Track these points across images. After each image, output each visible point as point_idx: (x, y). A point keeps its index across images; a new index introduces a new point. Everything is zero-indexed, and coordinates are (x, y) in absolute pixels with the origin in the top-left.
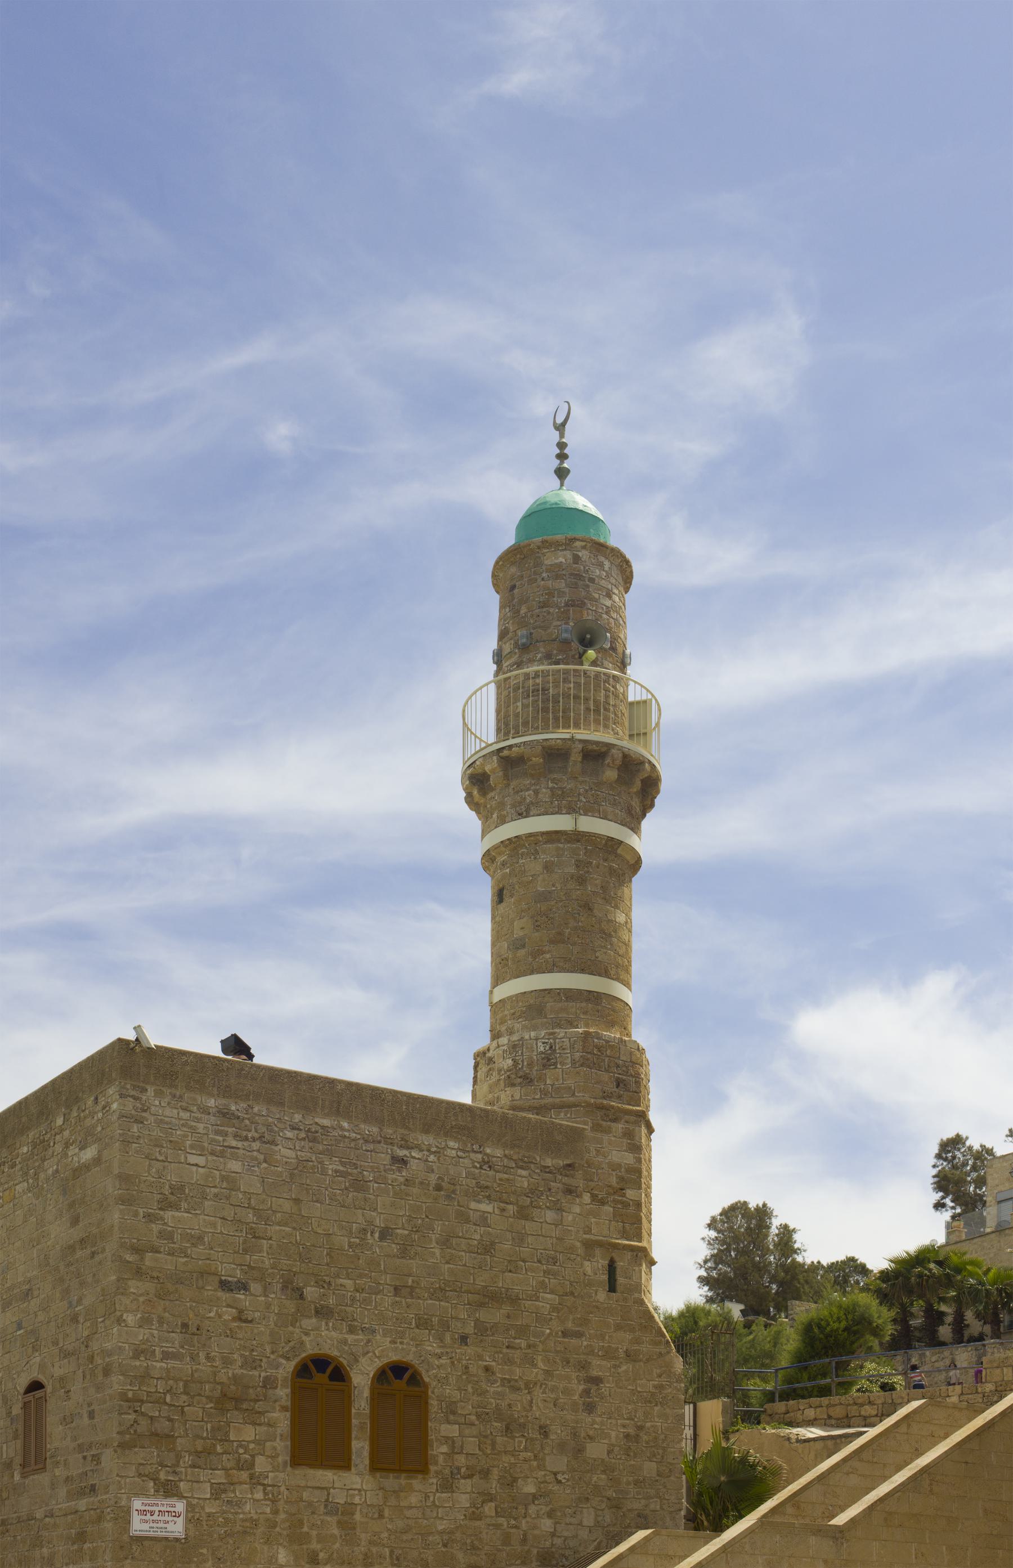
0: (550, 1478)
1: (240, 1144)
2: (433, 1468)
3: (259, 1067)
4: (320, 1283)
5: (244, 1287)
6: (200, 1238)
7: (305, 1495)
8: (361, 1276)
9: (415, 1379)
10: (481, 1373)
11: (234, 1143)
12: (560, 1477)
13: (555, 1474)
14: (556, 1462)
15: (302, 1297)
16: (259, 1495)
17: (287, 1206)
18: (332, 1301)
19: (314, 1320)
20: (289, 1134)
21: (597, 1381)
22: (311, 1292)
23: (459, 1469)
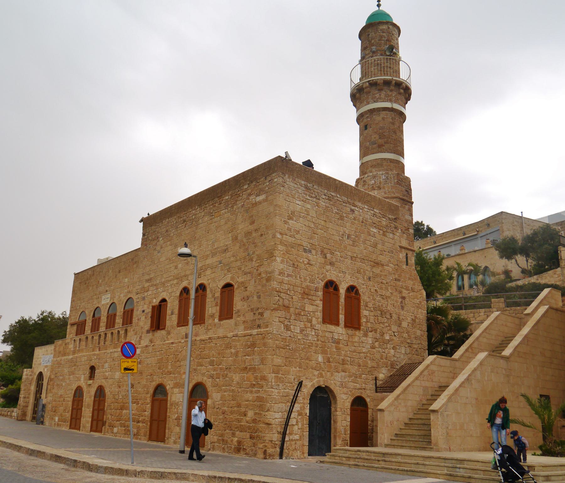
0: (393, 334)
1: (310, 199)
2: (362, 327)
3: (315, 171)
4: (332, 253)
5: (310, 252)
6: (299, 232)
7: (327, 334)
8: (342, 252)
9: (357, 292)
10: (374, 291)
11: (309, 198)
12: (395, 334)
13: (394, 332)
14: (394, 328)
15: (326, 258)
16: (313, 333)
17: (323, 223)
18: (334, 260)
19: (329, 266)
20: (324, 197)
21: (404, 298)
22: (329, 256)
23: (369, 328)
